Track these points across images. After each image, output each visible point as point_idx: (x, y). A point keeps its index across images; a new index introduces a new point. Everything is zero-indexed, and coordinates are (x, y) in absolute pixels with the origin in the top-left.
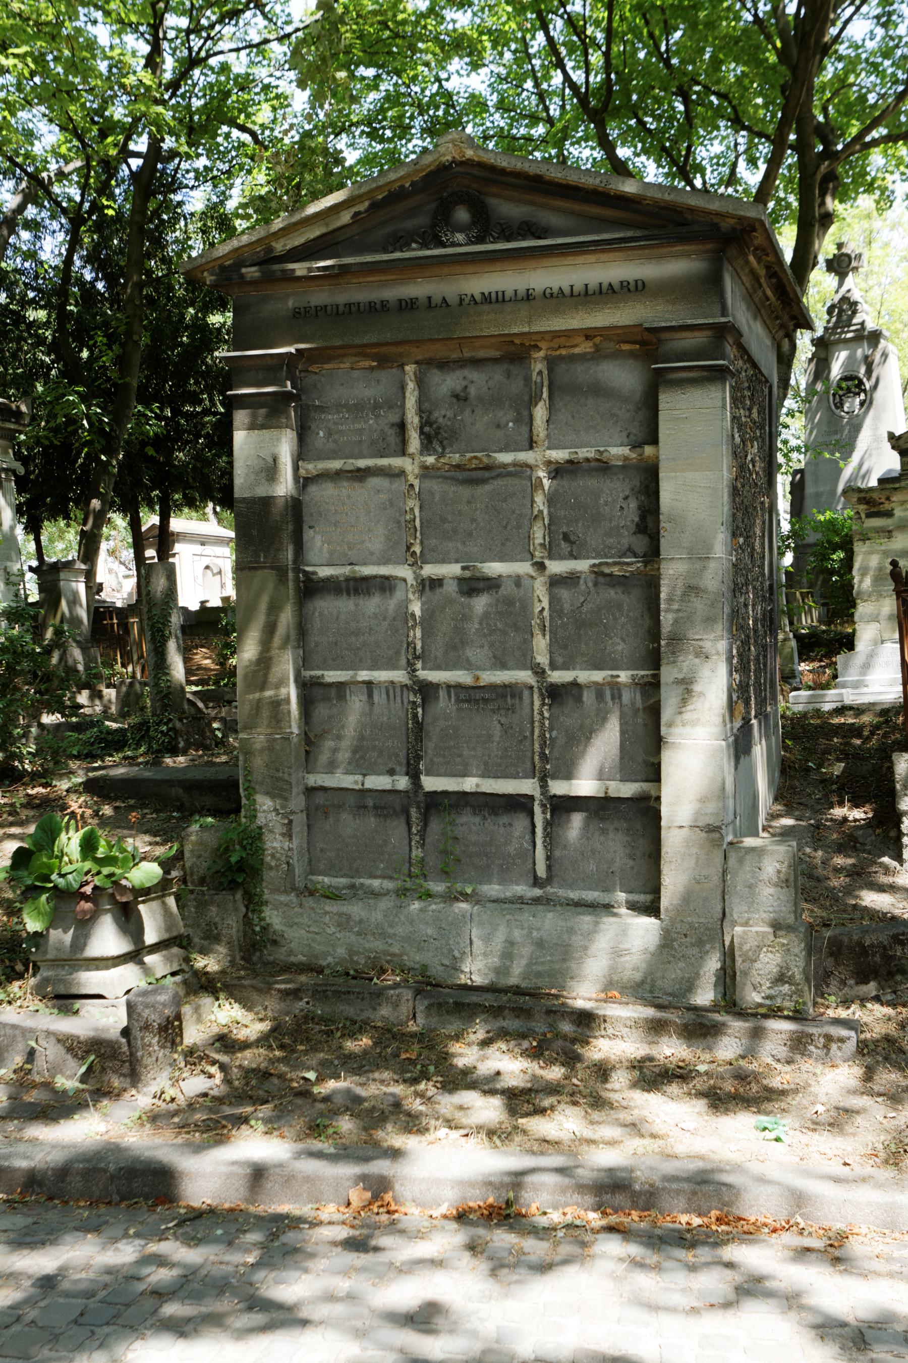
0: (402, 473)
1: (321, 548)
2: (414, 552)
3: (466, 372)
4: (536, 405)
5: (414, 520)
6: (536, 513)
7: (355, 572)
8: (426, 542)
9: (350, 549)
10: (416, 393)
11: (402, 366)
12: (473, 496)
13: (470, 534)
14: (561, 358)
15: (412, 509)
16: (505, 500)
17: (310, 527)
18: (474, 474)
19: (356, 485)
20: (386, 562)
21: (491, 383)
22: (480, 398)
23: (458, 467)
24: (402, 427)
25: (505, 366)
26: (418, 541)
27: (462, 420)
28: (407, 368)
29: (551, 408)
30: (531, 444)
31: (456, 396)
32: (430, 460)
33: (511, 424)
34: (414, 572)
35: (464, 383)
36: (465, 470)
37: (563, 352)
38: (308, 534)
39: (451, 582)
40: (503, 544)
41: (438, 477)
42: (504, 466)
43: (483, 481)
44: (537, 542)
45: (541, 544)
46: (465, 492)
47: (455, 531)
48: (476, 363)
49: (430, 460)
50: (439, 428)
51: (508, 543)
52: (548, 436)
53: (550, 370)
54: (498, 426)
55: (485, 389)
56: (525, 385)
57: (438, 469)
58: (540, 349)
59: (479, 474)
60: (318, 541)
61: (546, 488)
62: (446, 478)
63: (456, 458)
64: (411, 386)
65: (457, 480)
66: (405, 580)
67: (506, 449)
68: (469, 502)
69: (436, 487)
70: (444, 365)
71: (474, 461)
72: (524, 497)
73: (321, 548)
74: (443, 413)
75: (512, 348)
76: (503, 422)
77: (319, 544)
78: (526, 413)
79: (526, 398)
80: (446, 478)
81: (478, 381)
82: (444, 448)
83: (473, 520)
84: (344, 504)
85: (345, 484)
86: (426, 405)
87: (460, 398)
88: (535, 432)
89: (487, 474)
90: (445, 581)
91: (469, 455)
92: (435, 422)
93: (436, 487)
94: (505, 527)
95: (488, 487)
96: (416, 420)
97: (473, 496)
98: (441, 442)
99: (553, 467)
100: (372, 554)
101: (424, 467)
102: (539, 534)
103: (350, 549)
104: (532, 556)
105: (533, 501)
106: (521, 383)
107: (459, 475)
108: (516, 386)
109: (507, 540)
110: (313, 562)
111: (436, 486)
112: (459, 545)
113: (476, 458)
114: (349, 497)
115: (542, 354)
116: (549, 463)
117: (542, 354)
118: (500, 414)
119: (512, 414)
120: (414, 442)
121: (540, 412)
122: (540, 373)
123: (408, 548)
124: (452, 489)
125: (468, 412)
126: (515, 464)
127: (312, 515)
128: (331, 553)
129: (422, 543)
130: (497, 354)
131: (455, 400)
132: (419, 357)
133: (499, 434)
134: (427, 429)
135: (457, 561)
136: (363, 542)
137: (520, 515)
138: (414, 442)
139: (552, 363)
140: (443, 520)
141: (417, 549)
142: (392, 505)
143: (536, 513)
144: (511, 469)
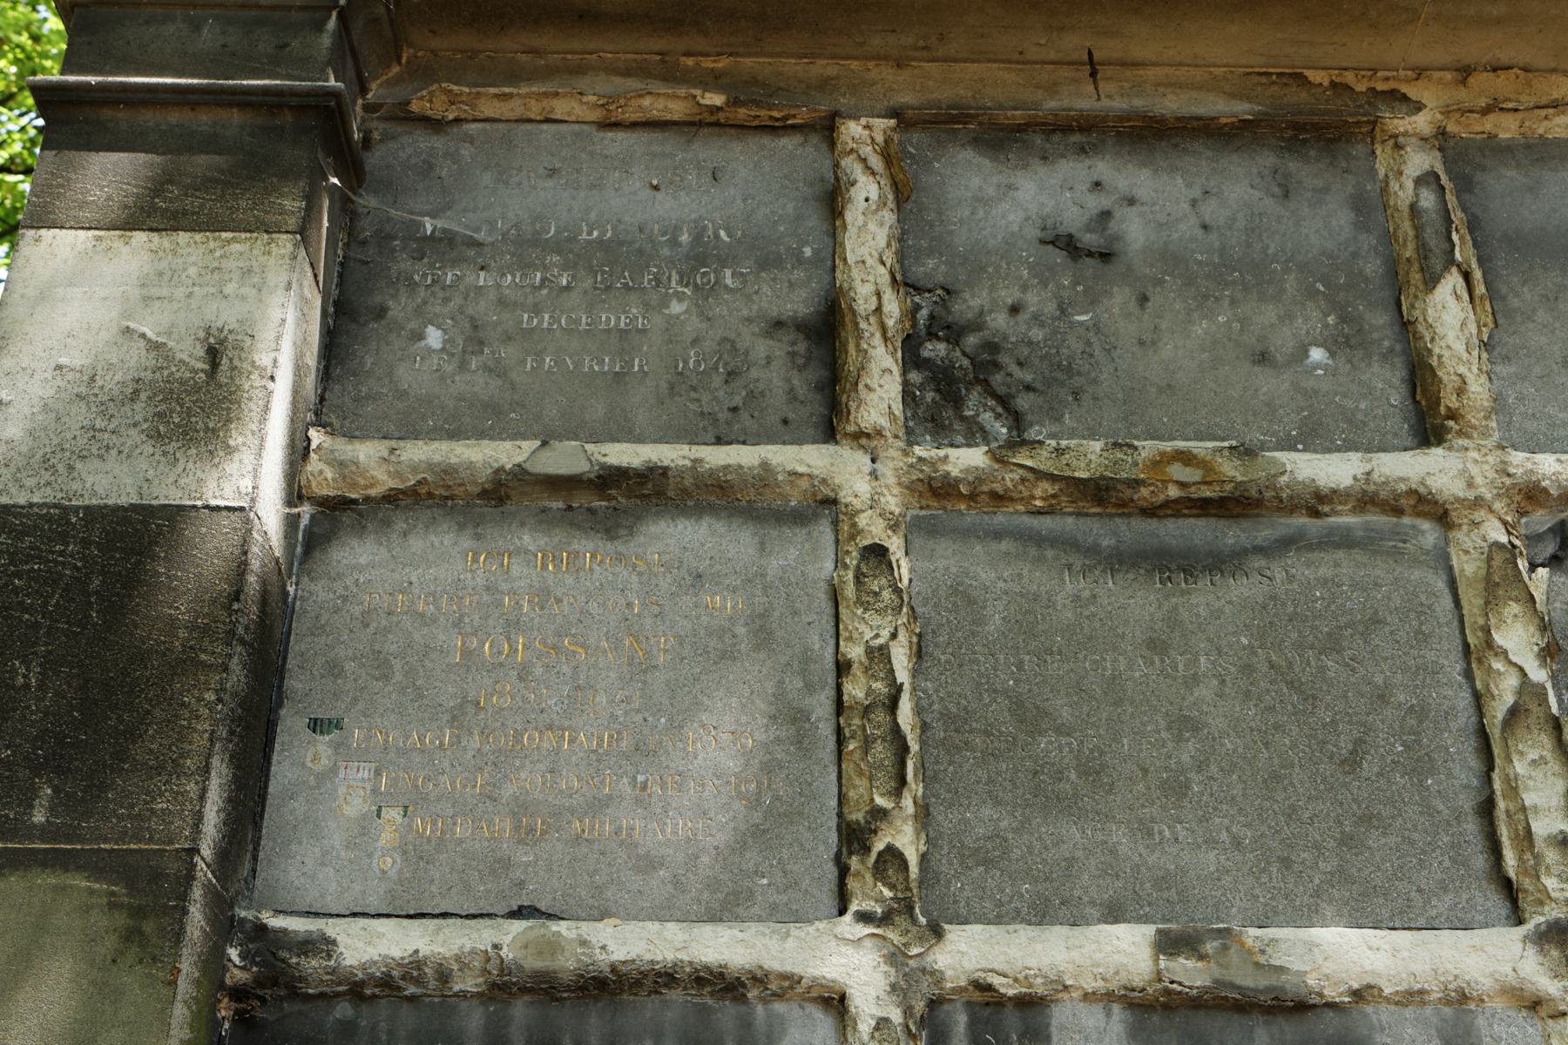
0: (825, 504)
1: (364, 829)
2: (892, 853)
3: (1102, 167)
4: (1431, 282)
5: (893, 704)
6: (1505, 692)
7: (554, 946)
8: (945, 819)
9: (526, 835)
10: (889, 217)
11: (827, 129)
12: (1172, 620)
13: (1176, 788)
14: (1493, 148)
15: (879, 656)
16: (1333, 644)
17: (316, 726)
18: (1172, 531)
19: (586, 546)
20: (726, 907)
21: (1209, 210)
22: (1171, 259)
23: (1099, 493)
24: (826, 331)
25: (1267, 159)
26: (908, 803)
27: (1096, 327)
28: (852, 130)
29: (1491, 299)
30: (1429, 424)
31: (1069, 245)
32: (966, 459)
33: (1317, 354)
34: (896, 958)
35: (1095, 203)
36: (1127, 508)
37: (1507, 128)
38: (298, 758)
39: (1092, 1017)
40: (1346, 840)
41: (998, 535)
42: (1318, 501)
43: (1221, 563)
44: (1542, 827)
46: (1136, 603)
47: (1093, 771)
48: (1148, 135)
49: (966, 459)
50: (992, 347)
51: (1374, 840)
52: (1498, 404)
53: (1465, 185)
54: (1263, 358)
55: (1188, 228)
56: (1362, 225)
57: (999, 498)
58: (1418, 107)
59: (1198, 532)
60: (352, 793)
61: (1539, 596)
62: (1039, 540)
63: (1091, 456)
64: (866, 190)
65: (1092, 550)
66: (836, 1003)
67: (1312, 438)
68: (1156, 646)
69: (986, 575)
70: (1006, 136)
71: (1177, 471)
72: (1422, 637)
73: (364, 829)
74: (1009, 295)
75: (1296, 96)
76: (1282, 341)
77: (355, 805)
78: (1379, 320)
79: (1372, 267)
80: (1039, 540)
81: (1155, 202)
82: (1017, 421)
83: (1184, 725)
84: (513, 625)
85: (527, 539)
86: (930, 268)
87: (1083, 251)
88: (1447, 376)
89: (1231, 535)
90: (1060, 1015)
91: (1148, 448)
92: (977, 325)
93: (986, 575)
94: (1352, 762)
95: (1243, 589)
96: (893, 307)
97: (1172, 620)
98: (1004, 401)
99: (1542, 520)
100: (648, 864)
101: (937, 490)
103: (526, 835)
105: (1476, 653)
106: (1343, 219)
107: (1102, 531)
108: (1321, 221)
109: (1367, 819)
110: (310, 899)
111: (991, 572)
112: (1120, 836)
113: (1186, 458)
114: (543, 596)
115: (1422, 122)
116: (1531, 495)
117: (1422, 122)
118: (1268, 314)
119: (1314, 320)
120: (881, 393)
121: (1449, 315)
122: (1428, 179)
123: (854, 837)
124: (1063, 589)
125: (1119, 299)
126: (1367, 498)
127: (334, 669)
128: (416, 853)
129: (924, 815)
130: (1244, 109)
131: (1058, 257)
132: (905, 98)
133: (1269, 384)
134: (935, 350)
135: (1114, 913)
136: (598, 806)
137: (1420, 712)
138: (881, 393)
139: (1463, 161)
140: (1030, 717)
141: (904, 837)
142: (763, 637)
143: (1505, 692)
144: (1347, 519)
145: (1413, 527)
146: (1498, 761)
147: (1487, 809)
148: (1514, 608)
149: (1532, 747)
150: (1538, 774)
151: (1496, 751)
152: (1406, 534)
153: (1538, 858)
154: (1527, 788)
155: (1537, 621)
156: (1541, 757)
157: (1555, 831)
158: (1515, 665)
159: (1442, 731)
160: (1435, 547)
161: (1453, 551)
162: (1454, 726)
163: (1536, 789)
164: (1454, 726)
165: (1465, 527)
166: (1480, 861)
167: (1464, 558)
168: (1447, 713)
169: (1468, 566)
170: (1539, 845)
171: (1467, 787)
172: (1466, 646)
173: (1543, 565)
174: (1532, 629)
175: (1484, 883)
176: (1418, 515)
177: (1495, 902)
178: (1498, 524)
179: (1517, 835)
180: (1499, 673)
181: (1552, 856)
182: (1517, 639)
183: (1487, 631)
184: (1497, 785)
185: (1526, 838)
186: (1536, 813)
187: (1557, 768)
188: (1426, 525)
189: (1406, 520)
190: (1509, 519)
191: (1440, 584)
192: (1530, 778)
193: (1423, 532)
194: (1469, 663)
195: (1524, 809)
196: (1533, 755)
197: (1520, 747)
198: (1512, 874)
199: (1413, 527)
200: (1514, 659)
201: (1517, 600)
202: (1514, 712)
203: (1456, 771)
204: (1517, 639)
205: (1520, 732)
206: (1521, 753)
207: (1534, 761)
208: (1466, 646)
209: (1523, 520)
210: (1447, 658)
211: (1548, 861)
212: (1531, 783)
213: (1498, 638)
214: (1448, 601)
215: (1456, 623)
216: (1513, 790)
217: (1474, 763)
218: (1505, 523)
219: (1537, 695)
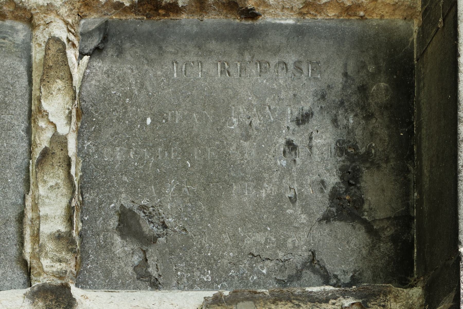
6: (43, 140)
44: (46, 229)
45: (58, 237)
61: (77, 77)
102: (51, 207)
104: (27, 270)
105: (33, 114)
143: (43, 140)
145: (12, 28)
146: (32, 187)
147: (21, 218)
148: (60, 84)
149: (53, 177)
150: (52, 195)
151: (32, 180)
152: (6, 33)
153: (41, 247)
154: (44, 204)
155: (71, 93)
156: (57, 184)
157: (55, 230)
158: (52, 123)
159: (6, 168)
160: (23, 42)
161: (33, 45)
162: (13, 165)
163: (50, 204)
164: (13, 165)
165: (42, 27)
166: (13, 251)
167: (38, 49)
168: (10, 156)
169: (38, 55)
170: (43, 239)
171: (13, 204)
172: (30, 110)
173: (87, 54)
174: (68, 98)
175: (14, 263)
176: (16, 18)
177: (18, 275)
178: (62, 24)
179: (34, 234)
180: (42, 129)
181: (50, 246)
182: (56, 106)
183: (39, 100)
184: (29, 203)
185: (36, 236)
186: (46, 219)
187: (65, 191)
188: (20, 26)
189: (8, 23)
190: (70, 20)
191: (22, 69)
192: (47, 197)
193: (17, 31)
194: (30, 124)
195: (39, 217)
196: (52, 182)
197: (45, 177)
198: (27, 257)
199: (12, 28)
200: (51, 119)
201: (62, 79)
202: (45, 153)
203: (9, 195)
204: (56, 106)
205: (47, 167)
206: (45, 182)
207: (51, 187)
208: (30, 110)
209: (82, 22)
210: (17, 119)
211: (48, 249)
212: (47, 201)
213: (45, 105)
214: (24, 81)
215: (27, 96)
216: (35, 207)
217: (21, 189)
218: (67, 23)
219: (61, 143)
